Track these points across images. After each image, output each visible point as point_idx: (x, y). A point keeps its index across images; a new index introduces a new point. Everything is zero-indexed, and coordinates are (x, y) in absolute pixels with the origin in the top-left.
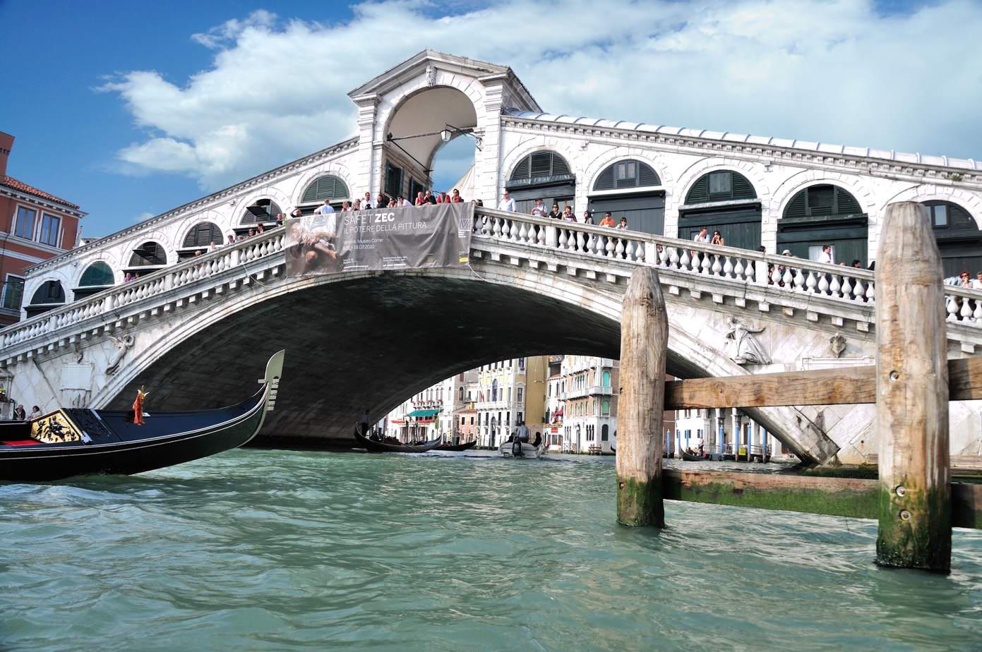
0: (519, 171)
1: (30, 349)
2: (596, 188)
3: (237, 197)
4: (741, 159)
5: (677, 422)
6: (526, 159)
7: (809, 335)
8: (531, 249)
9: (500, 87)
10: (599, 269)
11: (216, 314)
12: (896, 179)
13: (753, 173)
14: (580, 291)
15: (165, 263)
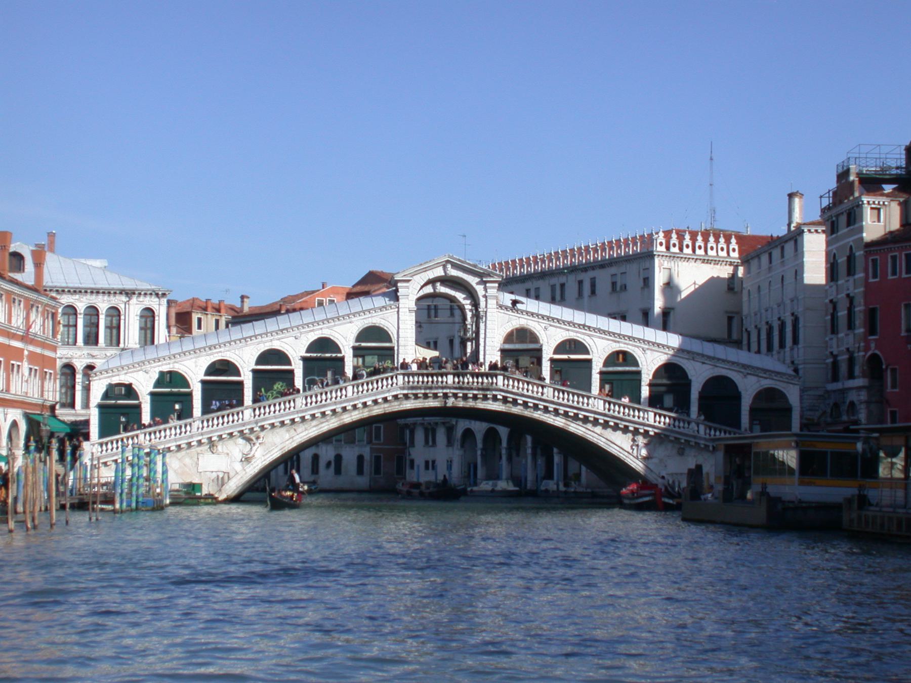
0: (509, 338)
1: (175, 444)
2: (555, 352)
3: (301, 333)
4: (633, 345)
5: (412, 450)
6: (512, 332)
7: (670, 446)
8: (540, 400)
9: (497, 285)
10: (575, 411)
11: (332, 423)
12: (703, 363)
13: (637, 353)
14: (564, 421)
15: (239, 375)
